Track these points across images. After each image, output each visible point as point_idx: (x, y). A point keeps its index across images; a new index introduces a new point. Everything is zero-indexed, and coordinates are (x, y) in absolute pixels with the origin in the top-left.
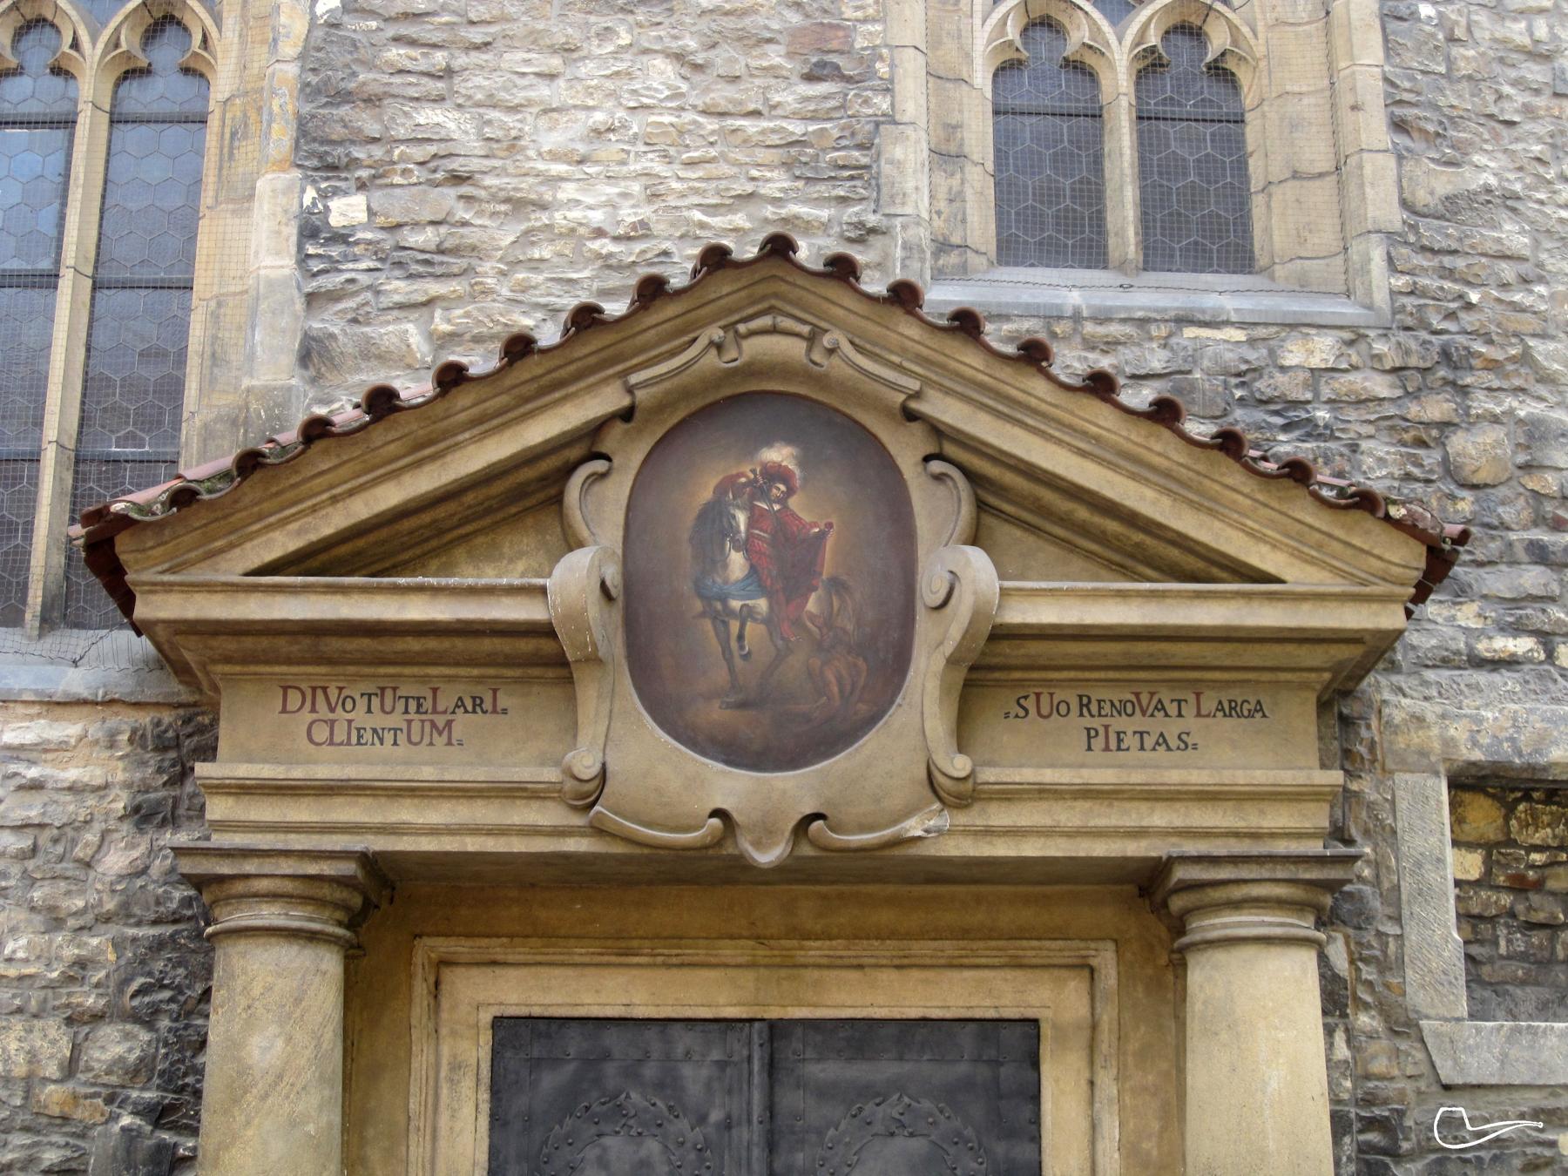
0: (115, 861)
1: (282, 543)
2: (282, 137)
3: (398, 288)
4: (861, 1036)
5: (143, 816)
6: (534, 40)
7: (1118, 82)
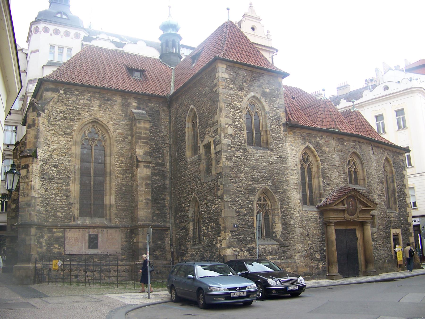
0: (319, 221)
1: (335, 204)
2: (321, 175)
4: (350, 230)
6: (332, 170)
7: (353, 173)
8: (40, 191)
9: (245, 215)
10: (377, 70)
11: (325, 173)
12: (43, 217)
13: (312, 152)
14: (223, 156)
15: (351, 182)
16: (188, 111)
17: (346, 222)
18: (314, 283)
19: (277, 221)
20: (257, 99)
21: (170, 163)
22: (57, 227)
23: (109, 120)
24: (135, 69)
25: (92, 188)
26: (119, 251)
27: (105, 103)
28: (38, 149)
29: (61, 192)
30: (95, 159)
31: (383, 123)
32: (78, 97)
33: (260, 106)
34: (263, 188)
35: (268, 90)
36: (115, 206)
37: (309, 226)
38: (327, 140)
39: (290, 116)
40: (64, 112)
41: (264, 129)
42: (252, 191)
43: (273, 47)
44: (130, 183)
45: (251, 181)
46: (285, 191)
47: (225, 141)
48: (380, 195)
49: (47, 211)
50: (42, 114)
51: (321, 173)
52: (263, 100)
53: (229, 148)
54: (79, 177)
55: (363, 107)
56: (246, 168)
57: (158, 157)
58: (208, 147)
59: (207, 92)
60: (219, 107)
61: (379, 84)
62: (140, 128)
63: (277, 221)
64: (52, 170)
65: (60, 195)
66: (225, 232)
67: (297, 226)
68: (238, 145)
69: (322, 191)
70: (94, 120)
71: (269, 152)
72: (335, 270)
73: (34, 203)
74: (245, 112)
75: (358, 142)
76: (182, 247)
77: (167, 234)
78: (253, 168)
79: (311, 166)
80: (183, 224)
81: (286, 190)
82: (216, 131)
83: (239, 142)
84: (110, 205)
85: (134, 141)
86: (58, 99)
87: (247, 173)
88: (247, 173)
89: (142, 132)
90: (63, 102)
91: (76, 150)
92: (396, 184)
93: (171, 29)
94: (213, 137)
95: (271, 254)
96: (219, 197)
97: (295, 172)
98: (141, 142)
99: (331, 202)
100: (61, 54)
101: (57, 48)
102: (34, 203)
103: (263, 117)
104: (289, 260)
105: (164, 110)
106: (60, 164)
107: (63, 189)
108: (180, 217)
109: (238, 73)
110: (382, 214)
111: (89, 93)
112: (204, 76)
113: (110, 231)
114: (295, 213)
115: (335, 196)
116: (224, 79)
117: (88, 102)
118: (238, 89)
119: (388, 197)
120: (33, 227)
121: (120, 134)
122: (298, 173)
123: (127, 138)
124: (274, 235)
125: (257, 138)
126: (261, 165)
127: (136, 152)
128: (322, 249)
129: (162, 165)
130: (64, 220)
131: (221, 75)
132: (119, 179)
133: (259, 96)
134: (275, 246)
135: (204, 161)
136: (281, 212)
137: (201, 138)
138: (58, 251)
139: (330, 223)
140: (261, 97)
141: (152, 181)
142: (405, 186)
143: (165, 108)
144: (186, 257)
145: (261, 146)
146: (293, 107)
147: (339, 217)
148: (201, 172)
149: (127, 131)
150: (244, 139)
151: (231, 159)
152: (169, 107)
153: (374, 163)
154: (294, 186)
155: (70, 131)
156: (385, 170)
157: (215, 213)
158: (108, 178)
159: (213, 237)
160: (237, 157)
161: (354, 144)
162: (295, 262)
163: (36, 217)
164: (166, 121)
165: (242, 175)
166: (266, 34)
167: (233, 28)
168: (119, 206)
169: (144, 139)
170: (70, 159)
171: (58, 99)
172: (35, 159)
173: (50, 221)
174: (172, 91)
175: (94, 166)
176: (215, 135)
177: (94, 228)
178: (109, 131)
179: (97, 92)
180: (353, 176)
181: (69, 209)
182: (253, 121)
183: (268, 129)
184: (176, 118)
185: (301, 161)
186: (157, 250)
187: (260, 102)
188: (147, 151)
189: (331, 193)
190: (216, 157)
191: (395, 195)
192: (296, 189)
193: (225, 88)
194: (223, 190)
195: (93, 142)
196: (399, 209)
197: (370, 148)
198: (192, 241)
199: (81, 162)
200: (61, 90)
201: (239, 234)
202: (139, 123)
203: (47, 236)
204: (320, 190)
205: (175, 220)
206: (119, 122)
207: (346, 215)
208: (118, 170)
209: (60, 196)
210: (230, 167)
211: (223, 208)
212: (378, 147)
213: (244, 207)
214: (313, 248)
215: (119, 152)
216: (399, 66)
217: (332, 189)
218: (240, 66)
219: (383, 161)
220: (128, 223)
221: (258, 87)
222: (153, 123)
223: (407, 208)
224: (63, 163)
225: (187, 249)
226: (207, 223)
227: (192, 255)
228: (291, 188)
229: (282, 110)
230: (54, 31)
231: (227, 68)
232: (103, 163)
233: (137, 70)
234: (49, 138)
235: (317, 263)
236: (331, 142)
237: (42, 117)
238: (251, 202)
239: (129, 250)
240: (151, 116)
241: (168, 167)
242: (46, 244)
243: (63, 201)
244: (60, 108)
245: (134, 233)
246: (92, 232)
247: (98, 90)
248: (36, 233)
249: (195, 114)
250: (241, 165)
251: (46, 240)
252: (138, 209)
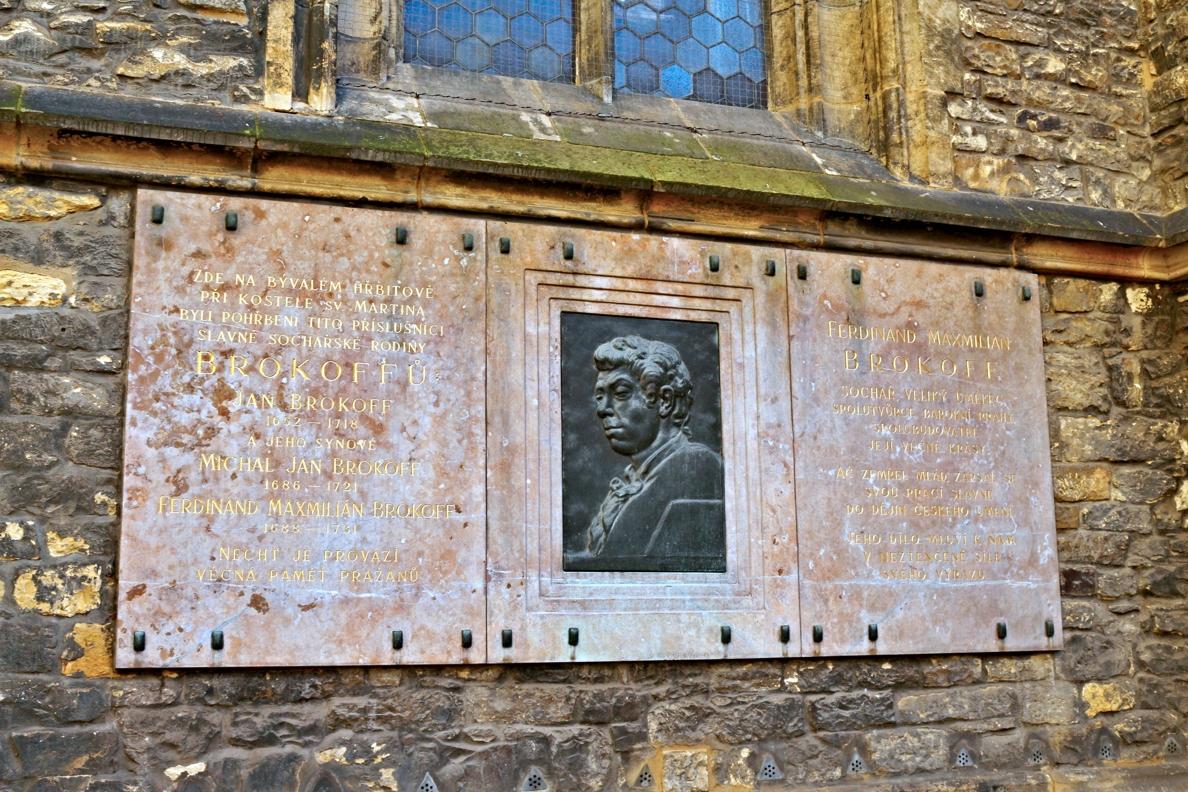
113: (896, 280)
177: (657, 205)
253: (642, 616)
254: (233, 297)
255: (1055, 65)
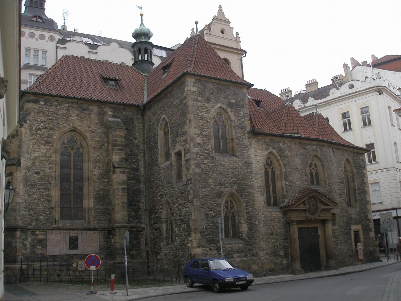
0: (282, 220)
1: (296, 205)
2: (284, 178)
3: (290, 188)
4: (312, 228)
5: (283, 218)
7: (314, 174)
8: (23, 197)
9: (214, 217)
10: (345, 66)
11: (287, 176)
12: (27, 221)
13: (276, 156)
14: (192, 164)
15: (312, 183)
16: (160, 119)
17: (308, 221)
18: (278, 278)
19: (243, 222)
20: (223, 109)
21: (145, 167)
22: (39, 230)
23: (86, 128)
24: (109, 76)
25: (72, 193)
26: (98, 251)
27: (83, 113)
28: (21, 158)
29: (42, 197)
30: (74, 165)
31: (349, 121)
32: (58, 108)
33: (226, 116)
34: (229, 192)
35: (233, 101)
36: (93, 209)
37: (273, 226)
38: (289, 144)
39: (254, 123)
40: (45, 122)
41: (230, 137)
42: (220, 195)
43: (242, 48)
44: (107, 187)
45: (218, 186)
46: (250, 194)
47: (195, 150)
48: (340, 194)
49: (30, 215)
50: (25, 124)
51: (284, 176)
52: (229, 110)
53: (198, 156)
54: (60, 182)
55: (330, 105)
56: (214, 174)
57: (133, 162)
58: (179, 154)
59: (177, 104)
60: (188, 118)
61: (345, 83)
62: (116, 136)
63: (243, 221)
64: (34, 177)
65: (42, 200)
66: (195, 233)
67: (261, 225)
68: (206, 153)
69: (285, 193)
70: (72, 129)
71: (234, 158)
72: (298, 266)
73: (19, 208)
74: (212, 122)
75: (319, 145)
76: (156, 246)
77: (143, 234)
78: (220, 173)
79: (274, 170)
80: (157, 225)
81: (251, 193)
82: (185, 141)
83: (206, 150)
84: (89, 208)
85: (110, 148)
86: (39, 109)
87: (214, 179)
88: (214, 179)
89: (117, 140)
90: (43, 112)
91: (56, 157)
92: (356, 183)
93: (143, 37)
94: (183, 146)
95: (238, 252)
96: (189, 201)
97: (259, 176)
98: (117, 149)
99: (293, 203)
100: (36, 56)
101: (32, 51)
102: (19, 208)
103: (229, 126)
104: (254, 258)
105: (138, 118)
106: (42, 171)
107: (45, 194)
108: (154, 218)
109: (206, 86)
110: (343, 212)
111: (67, 104)
112: (175, 88)
113: (89, 232)
114: (260, 214)
115: (296, 197)
116: (193, 92)
117: (66, 111)
118: (206, 101)
119: (349, 196)
120: (18, 231)
121: (98, 141)
122: (262, 177)
123: (104, 145)
124: (240, 235)
125: (224, 146)
126: (227, 170)
127: (112, 158)
128: (286, 246)
129: (137, 170)
130: (46, 224)
131: (190, 88)
132: (97, 184)
133: (225, 107)
134: (241, 245)
135: (175, 167)
136: (247, 213)
137: (172, 146)
138: (41, 252)
139: (292, 222)
140: (227, 108)
141: (127, 185)
142: (365, 184)
143: (139, 116)
144: (160, 256)
145: (227, 153)
146: (258, 115)
147: (302, 216)
148: (173, 177)
149: (103, 138)
150: (212, 147)
151: (200, 166)
152: (143, 115)
153: (335, 165)
154: (258, 189)
155: (49, 140)
156: (345, 170)
157: (186, 215)
158: (86, 184)
159: (184, 237)
160: (205, 164)
161: (315, 147)
162: (260, 259)
163: (20, 221)
164: (140, 129)
165: (210, 181)
166: (235, 36)
167: (201, 41)
168: (97, 209)
169: (119, 146)
170: (50, 166)
171: (39, 109)
172: (19, 168)
173: (33, 224)
174: (145, 100)
175: (73, 172)
176: (186, 144)
178: (87, 139)
179: (75, 103)
180: (315, 178)
181: (51, 213)
182: (220, 130)
183: (234, 137)
184: (149, 126)
185: (265, 166)
186: (133, 250)
187: (226, 112)
188: (122, 158)
189: (294, 194)
190: (186, 164)
191: (355, 193)
192: (260, 191)
193: (194, 101)
194: (193, 195)
195: (72, 149)
196: (360, 207)
197: (331, 150)
198: (165, 241)
199: (61, 168)
200: (41, 101)
201: (208, 235)
202: (115, 131)
203: (31, 238)
204: (283, 192)
205: (150, 221)
206: (96, 130)
207: (308, 214)
208: (96, 175)
209: (42, 201)
210: (199, 174)
211: (193, 211)
212: (339, 149)
213: (212, 210)
214: (277, 246)
215: (96, 159)
216: (366, 62)
217: (295, 191)
218: (208, 79)
219: (343, 162)
220: (106, 225)
221: (225, 98)
222: (128, 130)
223: (368, 205)
224: (44, 170)
225: (161, 248)
226: (179, 225)
227: (166, 254)
228: (255, 191)
229: (247, 118)
230: (30, 35)
231: (195, 81)
232: (82, 169)
233: (112, 80)
234: (31, 147)
235: (281, 259)
236: (293, 146)
237: (25, 128)
238: (219, 205)
239: (107, 249)
240: (126, 124)
241: (142, 172)
242: (30, 245)
243: (45, 205)
244: (41, 118)
245: (111, 234)
246: (72, 234)
247: (76, 101)
248: (21, 236)
249: (166, 123)
250: (209, 171)
251: (30, 242)
252: (114, 211)
253: (73, 252)
254: (53, 237)
255: (102, 217)
